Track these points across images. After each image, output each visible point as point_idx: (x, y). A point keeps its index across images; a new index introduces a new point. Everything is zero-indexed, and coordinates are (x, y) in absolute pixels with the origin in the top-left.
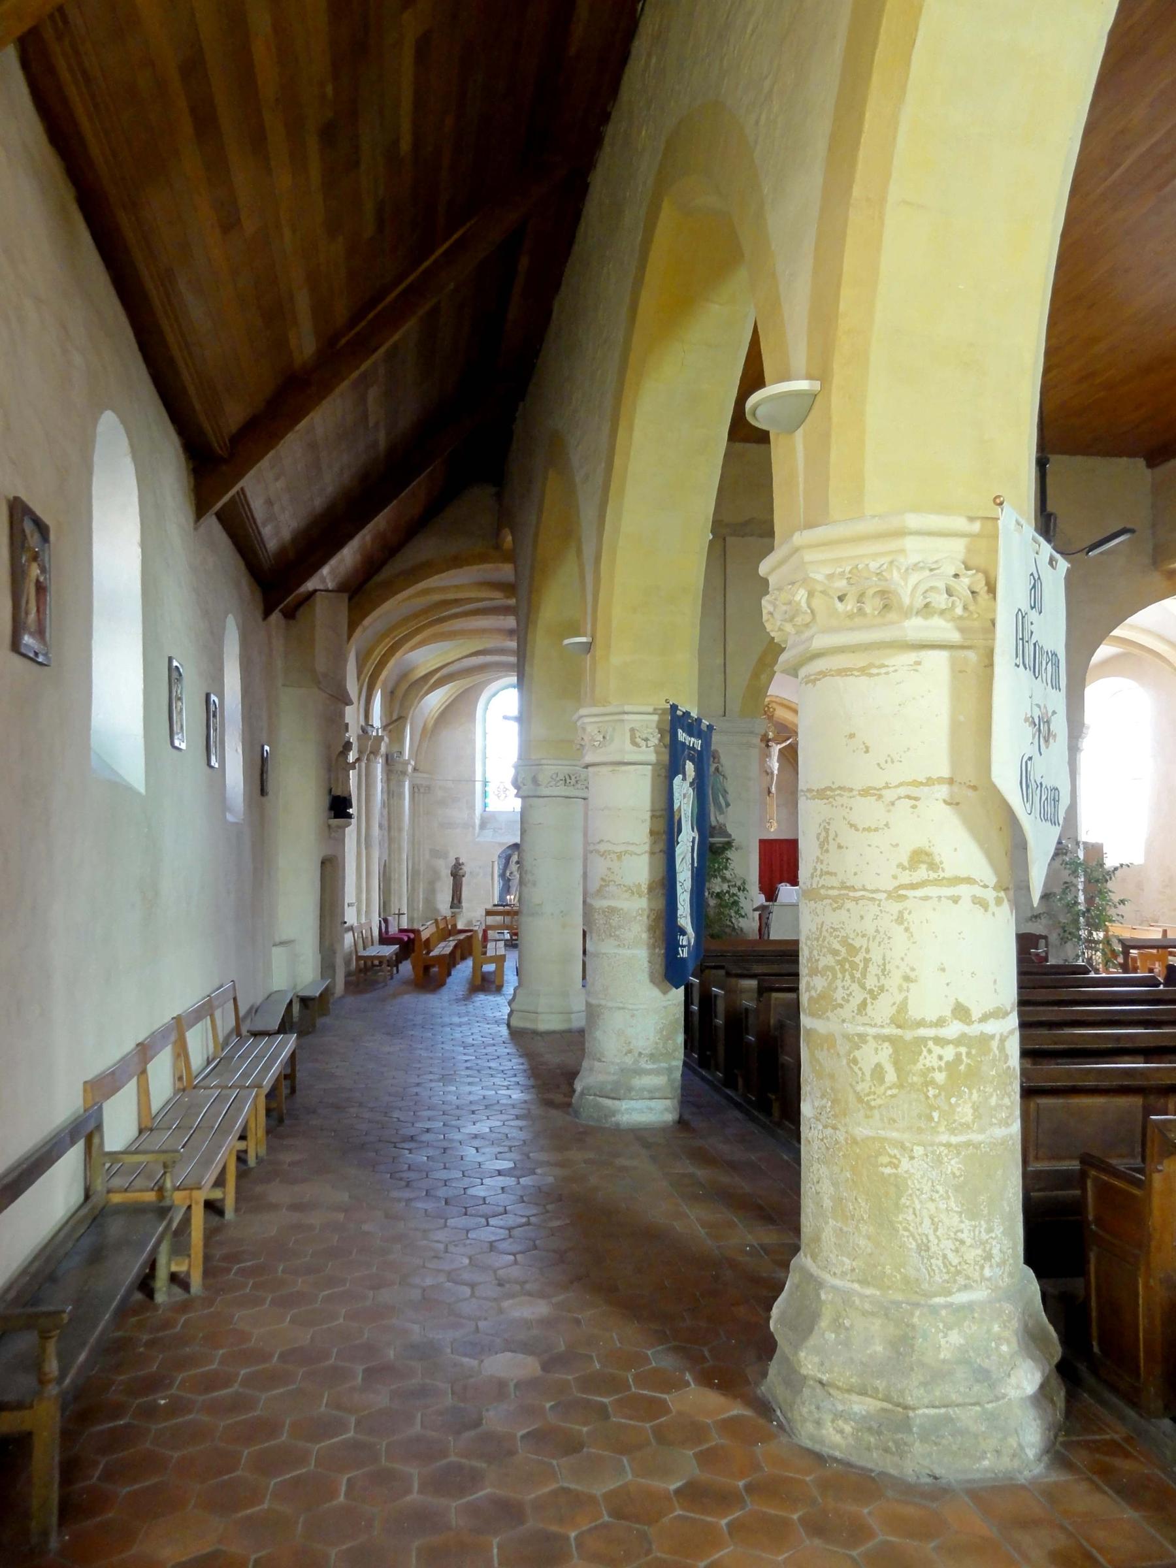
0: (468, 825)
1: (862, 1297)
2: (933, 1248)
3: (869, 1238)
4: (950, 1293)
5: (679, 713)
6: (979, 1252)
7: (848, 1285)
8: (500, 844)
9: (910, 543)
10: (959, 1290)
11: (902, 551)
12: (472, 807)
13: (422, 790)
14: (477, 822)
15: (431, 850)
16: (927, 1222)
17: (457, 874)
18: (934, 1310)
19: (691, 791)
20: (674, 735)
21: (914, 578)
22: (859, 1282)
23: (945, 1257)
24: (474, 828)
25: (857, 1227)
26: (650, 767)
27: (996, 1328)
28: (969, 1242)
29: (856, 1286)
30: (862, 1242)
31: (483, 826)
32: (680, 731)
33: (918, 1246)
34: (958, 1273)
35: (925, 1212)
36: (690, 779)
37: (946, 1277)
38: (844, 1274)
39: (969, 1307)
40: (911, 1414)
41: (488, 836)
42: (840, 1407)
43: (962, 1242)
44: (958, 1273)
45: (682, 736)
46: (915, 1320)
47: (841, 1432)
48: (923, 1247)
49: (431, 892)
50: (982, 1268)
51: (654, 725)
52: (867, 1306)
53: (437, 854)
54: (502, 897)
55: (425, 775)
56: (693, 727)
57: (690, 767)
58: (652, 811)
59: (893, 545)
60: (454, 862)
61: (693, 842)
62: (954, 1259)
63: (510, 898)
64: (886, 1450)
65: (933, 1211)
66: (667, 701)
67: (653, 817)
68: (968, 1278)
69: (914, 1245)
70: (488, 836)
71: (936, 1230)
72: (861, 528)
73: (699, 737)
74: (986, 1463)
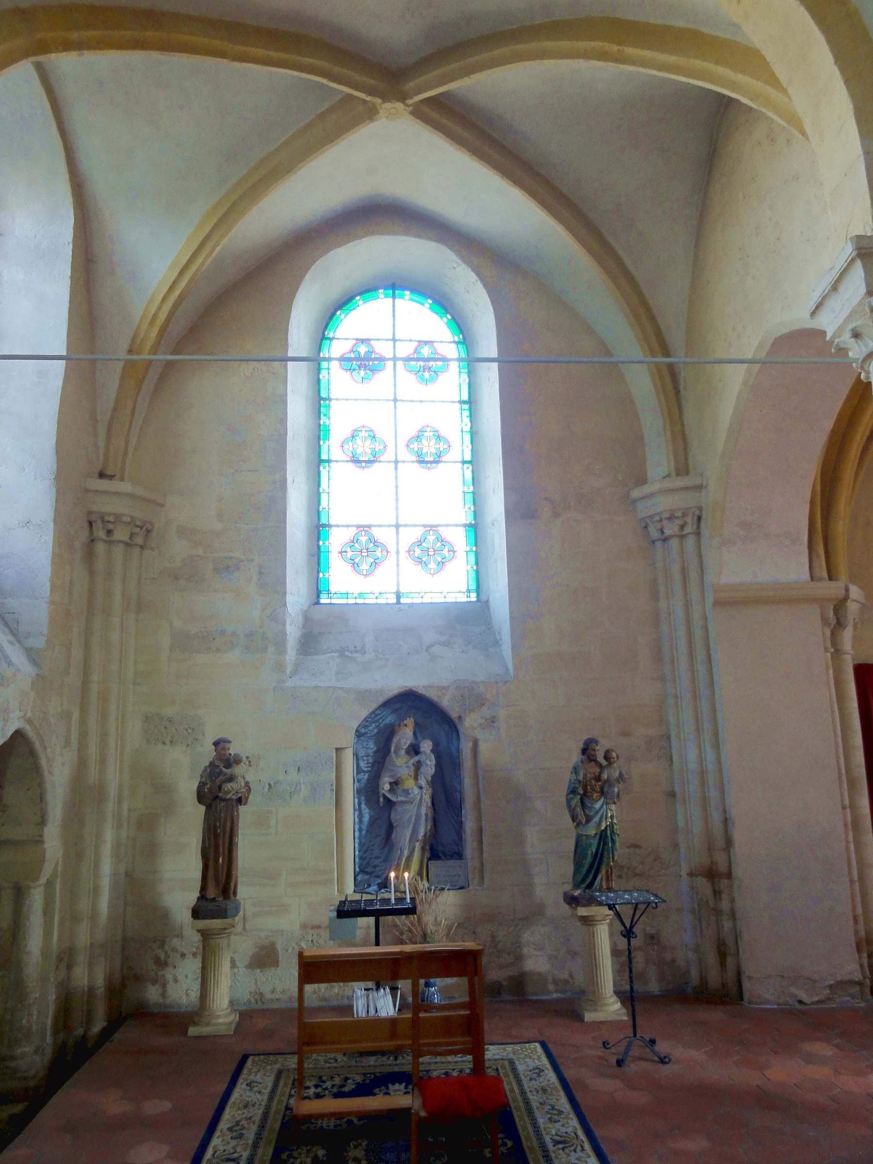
0: (263, 640)
8: (361, 695)
12: (275, 585)
13: (121, 534)
14: (293, 632)
15: (147, 719)
17: (220, 796)
24: (281, 647)
31: (310, 642)
41: (325, 672)
49: (143, 848)
53: (161, 729)
54: (370, 869)
55: (125, 487)
60: (207, 753)
63: (403, 878)
70: (325, 672)
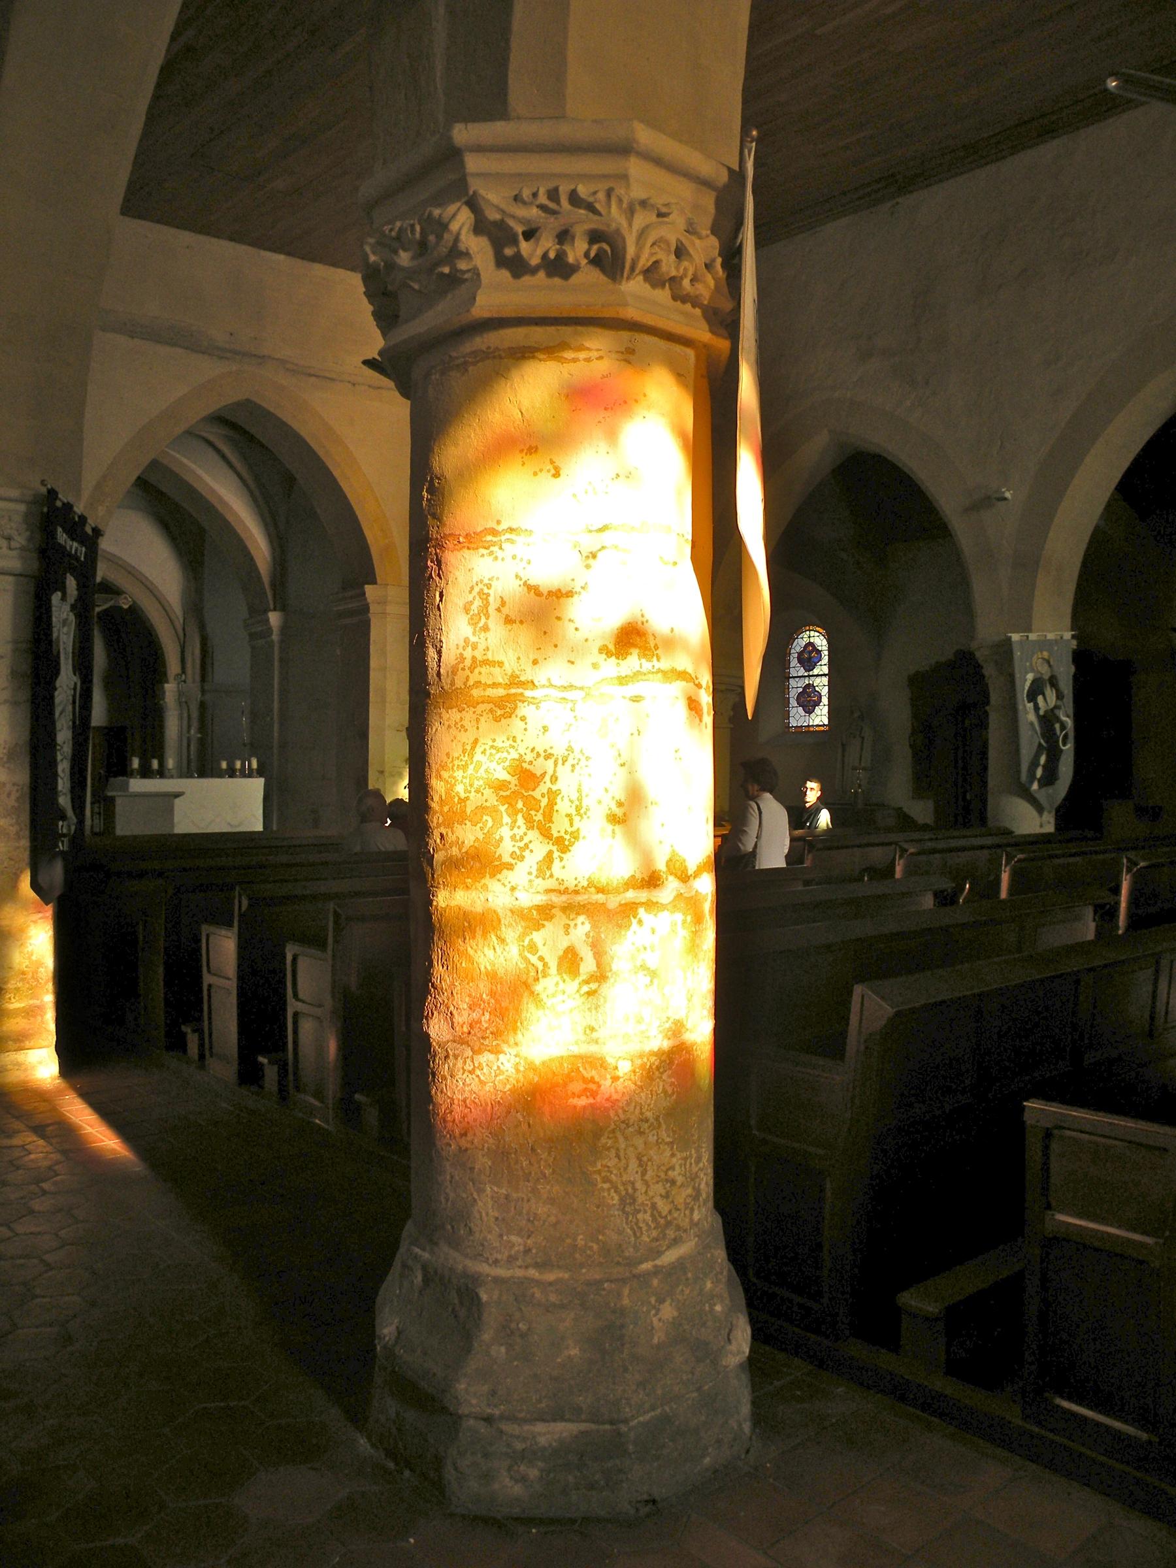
1: (545, 1286)
2: (641, 1198)
3: (551, 1201)
4: (659, 1253)
5: (59, 504)
6: (690, 1191)
7: (519, 1273)
9: (635, 167)
10: (668, 1248)
11: (625, 177)
16: (633, 1165)
18: (643, 1279)
19: (72, 617)
20: (52, 535)
21: (641, 219)
22: (536, 1265)
23: (654, 1206)
25: (534, 1190)
26: (11, 579)
27: (709, 1285)
28: (680, 1180)
29: (533, 1273)
30: (542, 1210)
32: (60, 529)
33: (622, 1200)
34: (668, 1224)
35: (631, 1153)
36: (71, 599)
37: (654, 1233)
38: (511, 1259)
39: (680, 1266)
40: (624, 1428)
42: (519, 1446)
43: (673, 1182)
44: (668, 1224)
45: (62, 537)
46: (626, 1302)
47: (524, 1479)
48: (628, 1200)
50: (692, 1210)
51: (18, 518)
52: (553, 1298)
56: (77, 527)
57: (71, 583)
58: (15, 642)
59: (607, 165)
61: (75, 689)
62: (663, 1206)
64: (591, 1487)
65: (641, 1147)
66: (43, 483)
67: (15, 651)
68: (678, 1228)
69: (616, 1201)
71: (644, 1173)
72: (565, 131)
73: (82, 543)
74: (707, 1460)
